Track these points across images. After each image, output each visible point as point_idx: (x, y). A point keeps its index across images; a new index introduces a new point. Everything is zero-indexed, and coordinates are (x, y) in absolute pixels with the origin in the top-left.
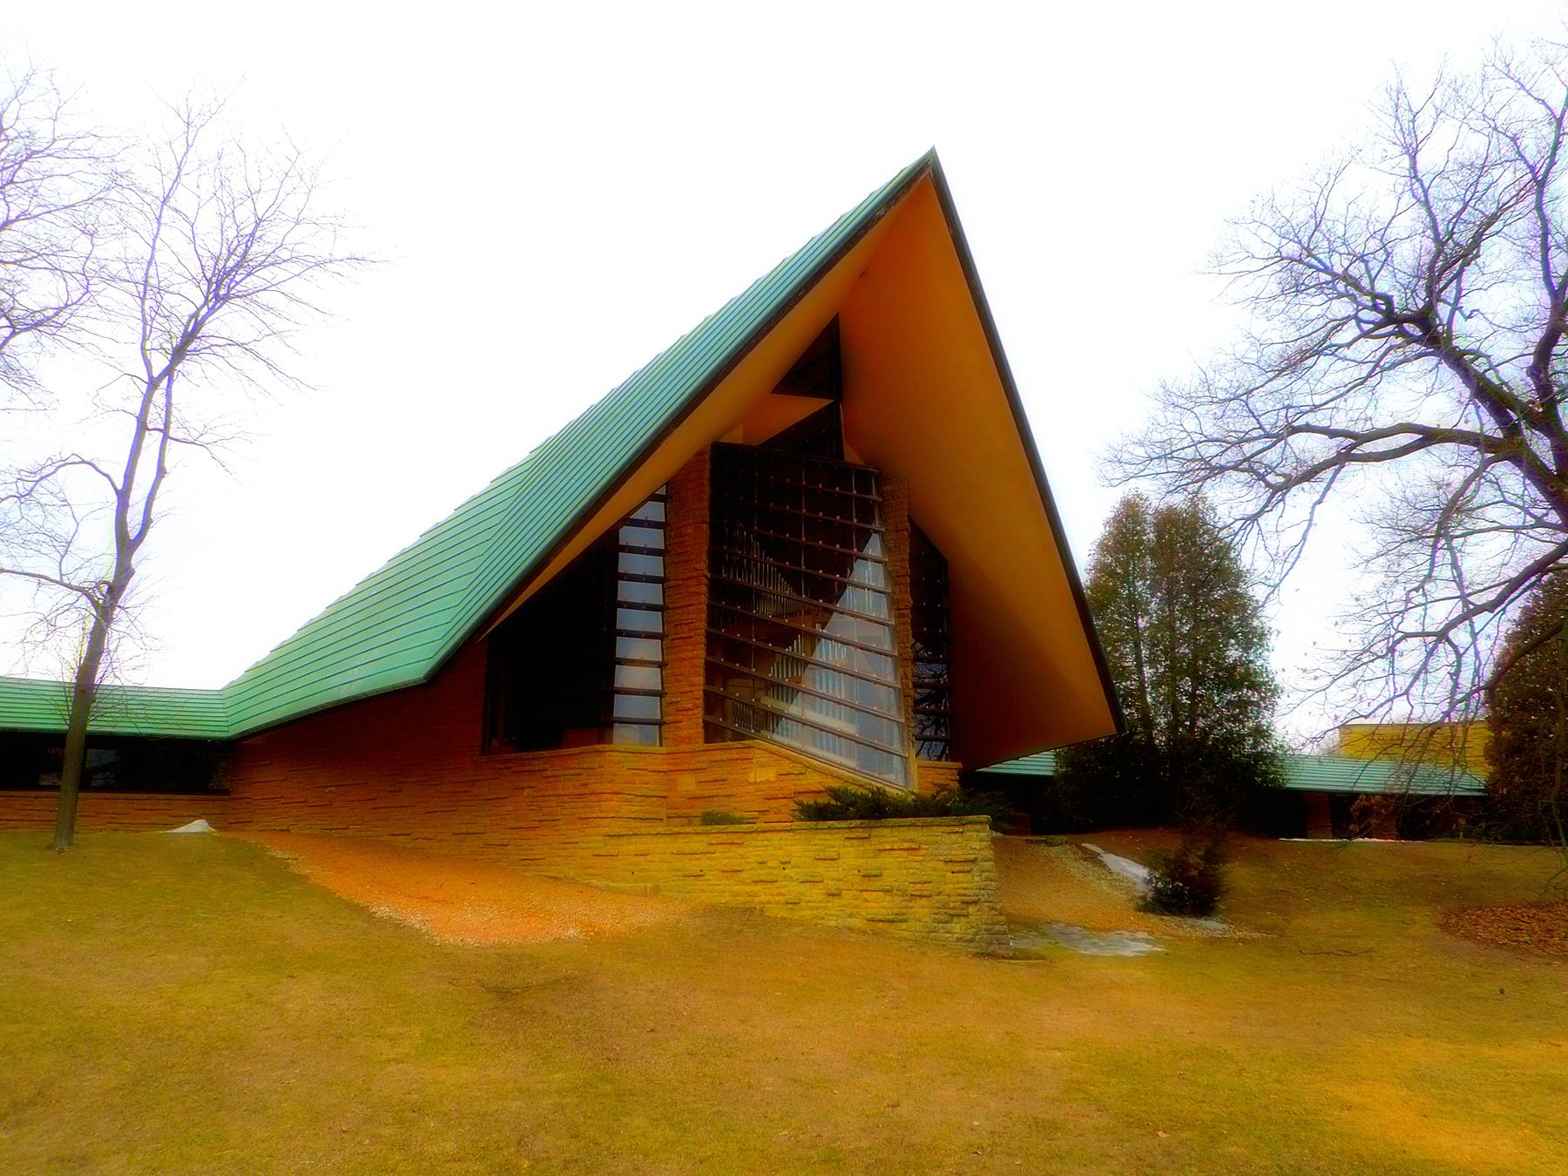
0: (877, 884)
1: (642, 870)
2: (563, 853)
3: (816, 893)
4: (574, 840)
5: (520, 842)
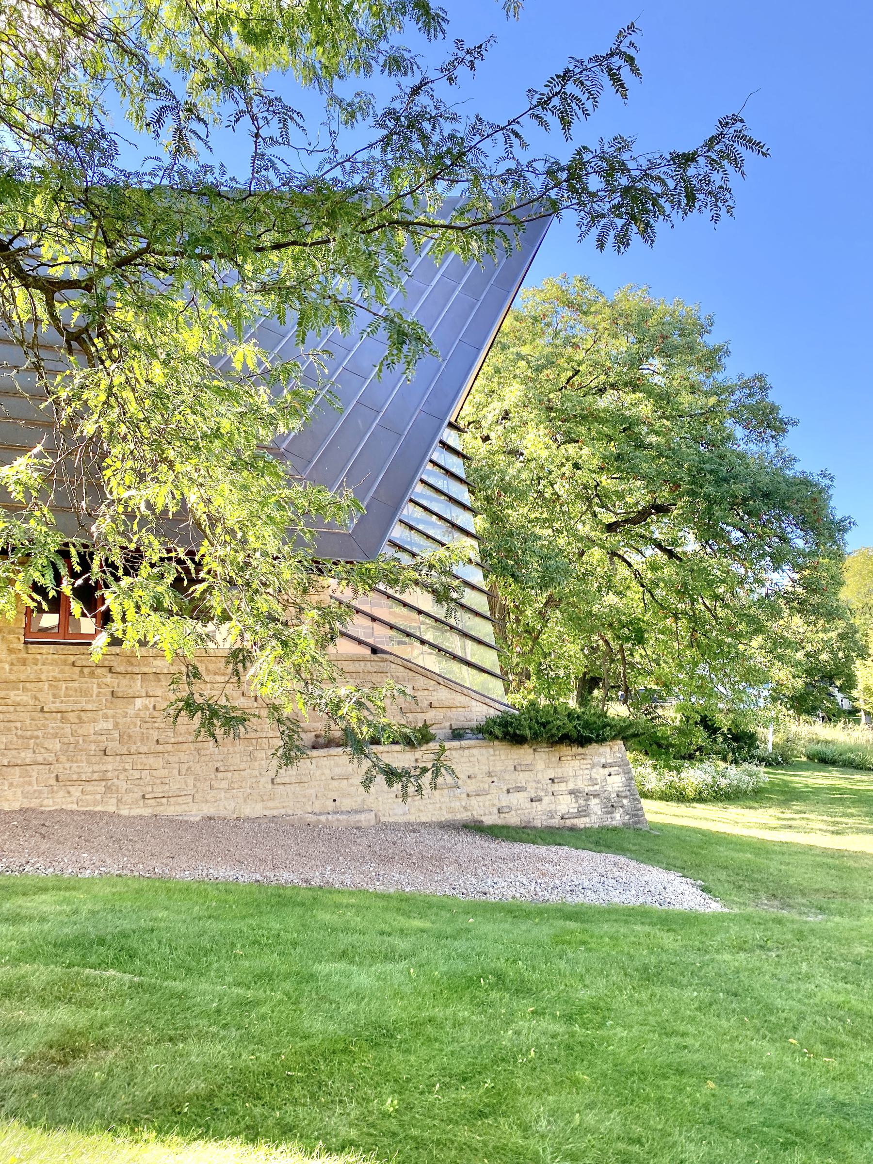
0: (563, 787)
1: (343, 796)
2: (224, 784)
3: (519, 799)
4: (242, 767)
5: (137, 775)
